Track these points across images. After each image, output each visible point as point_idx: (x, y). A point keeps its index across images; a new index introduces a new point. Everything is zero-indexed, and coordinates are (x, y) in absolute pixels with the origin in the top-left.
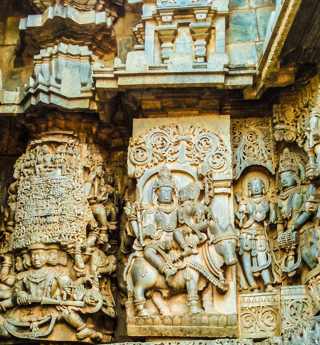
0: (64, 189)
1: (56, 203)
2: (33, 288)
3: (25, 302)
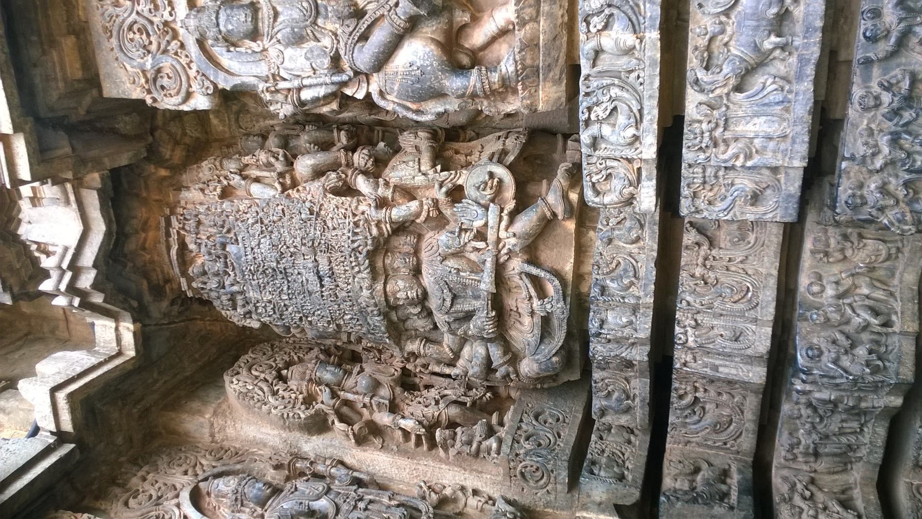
0: (262, 240)
1: (291, 256)
2: (464, 306)
3: (491, 322)
